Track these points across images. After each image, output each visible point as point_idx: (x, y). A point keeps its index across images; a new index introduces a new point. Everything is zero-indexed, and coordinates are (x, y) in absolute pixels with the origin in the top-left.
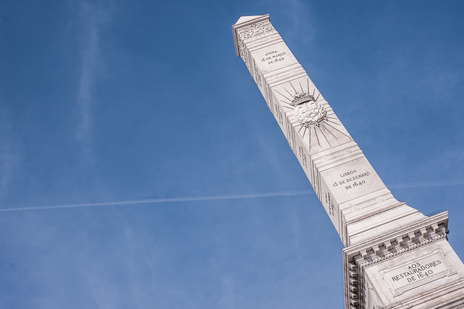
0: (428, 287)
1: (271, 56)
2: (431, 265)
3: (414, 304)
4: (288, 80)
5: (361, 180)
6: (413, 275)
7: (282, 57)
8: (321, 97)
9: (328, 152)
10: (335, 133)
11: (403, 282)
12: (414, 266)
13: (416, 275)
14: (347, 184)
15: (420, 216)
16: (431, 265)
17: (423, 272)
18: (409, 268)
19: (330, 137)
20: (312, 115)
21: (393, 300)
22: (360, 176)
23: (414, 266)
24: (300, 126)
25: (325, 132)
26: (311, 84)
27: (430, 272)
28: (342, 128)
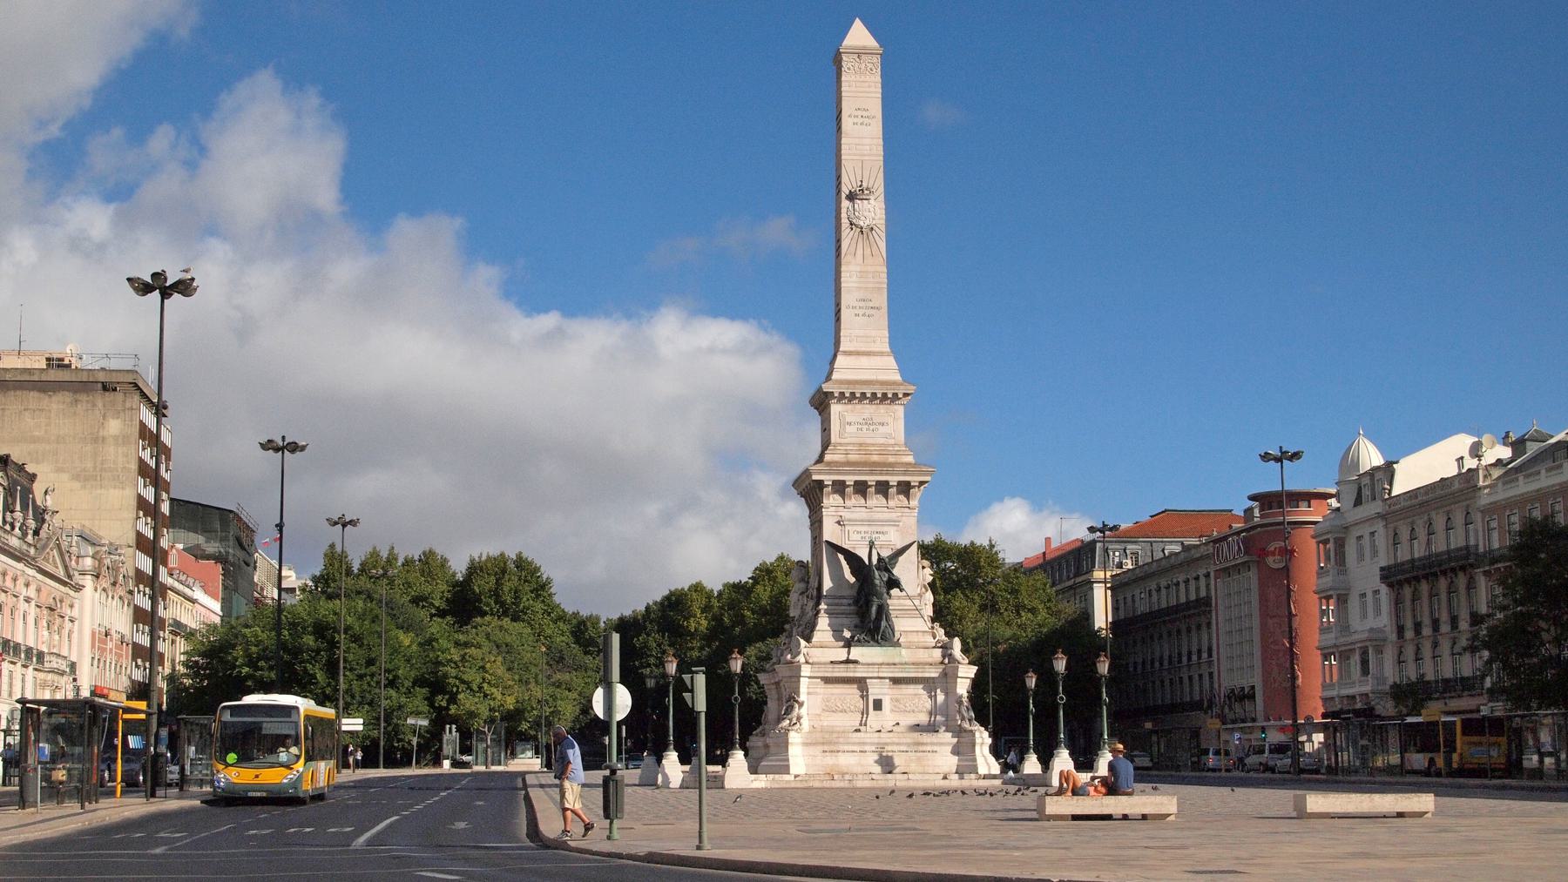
0: (869, 441)
1: (860, 113)
2: (880, 424)
7: (870, 121)
9: (858, 269)
13: (865, 427)
15: (898, 377)
16: (880, 424)
17: (871, 428)
19: (868, 251)
21: (839, 441)
28: (883, 245)
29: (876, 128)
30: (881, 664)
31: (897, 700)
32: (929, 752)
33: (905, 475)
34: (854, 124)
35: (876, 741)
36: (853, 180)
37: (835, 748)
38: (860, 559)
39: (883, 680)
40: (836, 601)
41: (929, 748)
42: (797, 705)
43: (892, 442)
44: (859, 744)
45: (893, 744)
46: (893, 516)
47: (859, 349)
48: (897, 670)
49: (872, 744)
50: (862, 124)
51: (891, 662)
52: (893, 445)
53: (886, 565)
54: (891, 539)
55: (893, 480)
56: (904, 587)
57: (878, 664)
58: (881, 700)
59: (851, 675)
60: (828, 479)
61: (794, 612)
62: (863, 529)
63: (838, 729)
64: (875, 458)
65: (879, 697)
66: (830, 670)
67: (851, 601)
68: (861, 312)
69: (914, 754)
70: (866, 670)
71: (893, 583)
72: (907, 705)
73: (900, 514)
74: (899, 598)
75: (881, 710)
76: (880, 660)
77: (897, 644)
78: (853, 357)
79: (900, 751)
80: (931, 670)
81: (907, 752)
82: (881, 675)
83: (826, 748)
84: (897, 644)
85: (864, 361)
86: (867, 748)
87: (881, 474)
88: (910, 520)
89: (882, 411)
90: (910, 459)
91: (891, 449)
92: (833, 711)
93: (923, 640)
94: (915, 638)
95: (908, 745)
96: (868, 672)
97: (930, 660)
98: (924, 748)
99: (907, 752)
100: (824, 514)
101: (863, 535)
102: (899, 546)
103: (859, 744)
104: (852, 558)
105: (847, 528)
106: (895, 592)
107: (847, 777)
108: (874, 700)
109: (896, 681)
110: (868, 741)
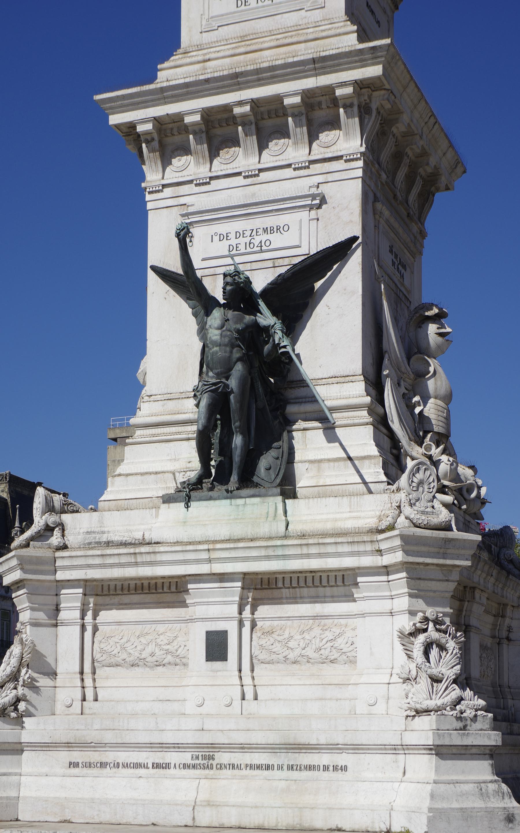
32: (326, 768)
35: (190, 738)
41: (325, 759)
44: (151, 746)
45: (230, 747)
48: (254, 553)
58: (224, 634)
66: (98, 561)
69: (285, 773)
75: (227, 660)
76: (224, 532)
79: (252, 767)
81: (268, 767)
82: (218, 568)
83: (77, 756)
99: (268, 767)
101: (233, 242)
103: (151, 746)
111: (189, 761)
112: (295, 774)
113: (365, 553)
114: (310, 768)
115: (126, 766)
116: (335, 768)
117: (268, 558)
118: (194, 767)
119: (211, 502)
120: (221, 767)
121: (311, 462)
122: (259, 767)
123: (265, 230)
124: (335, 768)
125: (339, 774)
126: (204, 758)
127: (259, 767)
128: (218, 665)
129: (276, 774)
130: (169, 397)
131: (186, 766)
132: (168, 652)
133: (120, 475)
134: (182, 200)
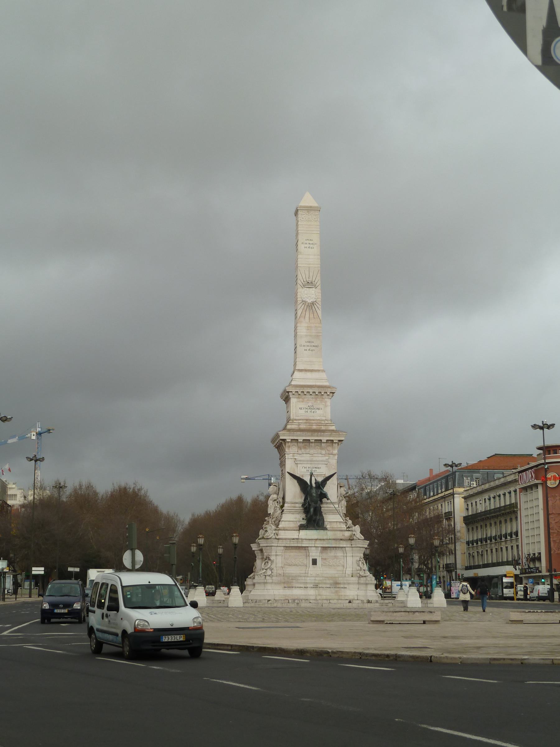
0: (311, 418)
1: (308, 242)
3: (301, 424)
4: (309, 266)
5: (314, 348)
6: (308, 410)
8: (319, 287)
10: (315, 314)
11: (302, 412)
12: (311, 406)
13: (309, 410)
14: (306, 348)
17: (313, 411)
18: (309, 406)
19: (312, 316)
20: (310, 298)
22: (314, 346)
23: (311, 406)
24: (301, 301)
25: (311, 311)
26: (319, 278)
27: (315, 412)
29: (316, 250)
30: (316, 540)
31: (325, 559)
33: (330, 436)
34: (305, 247)
35: (313, 581)
36: (304, 277)
37: (290, 586)
38: (305, 482)
39: (317, 548)
40: (293, 505)
42: (270, 562)
43: (324, 418)
46: (324, 458)
47: (306, 368)
48: (325, 543)
49: (311, 583)
50: (309, 247)
51: (322, 538)
52: (324, 420)
53: (321, 485)
54: (322, 472)
55: (324, 439)
56: (329, 498)
57: (315, 540)
58: (316, 560)
59: (300, 545)
60: (288, 438)
61: (270, 511)
62: (309, 466)
63: (293, 575)
64: (314, 427)
65: (315, 558)
67: (301, 505)
68: (308, 348)
69: (334, 589)
70: (308, 543)
71: (324, 496)
72: (330, 562)
73: (328, 458)
74: (327, 503)
75: (316, 565)
76: (316, 537)
77: (325, 529)
78: (303, 373)
79: (326, 587)
80: (343, 543)
81: (330, 588)
82: (316, 545)
83: (286, 585)
84: (325, 529)
85: (309, 375)
86: (308, 586)
87: (317, 436)
88: (333, 461)
89: (319, 402)
90: (333, 428)
91: (323, 422)
92: (290, 565)
93: (339, 526)
94: (335, 526)
95: (331, 584)
96: (309, 544)
97: (343, 538)
98: (340, 586)
99: (330, 588)
100: (286, 457)
102: (327, 475)
104: (300, 481)
105: (299, 465)
106: (324, 500)
107: (296, 601)
108: (313, 559)
109: (324, 548)
110: (309, 581)
111: (312, 586)
112: (336, 589)
113: (348, 544)
114: (339, 588)
115: (298, 587)
116: (344, 588)
117: (328, 544)
118: (313, 588)
119: (312, 531)
120: (320, 587)
121: (329, 522)
122: (328, 587)
123: (315, 468)
124: (344, 588)
125: (345, 589)
126: (316, 586)
127: (328, 587)
128: (315, 566)
129: (332, 589)
130: (291, 503)
131: (312, 587)
132: (302, 563)
133: (283, 521)
134: (295, 457)
